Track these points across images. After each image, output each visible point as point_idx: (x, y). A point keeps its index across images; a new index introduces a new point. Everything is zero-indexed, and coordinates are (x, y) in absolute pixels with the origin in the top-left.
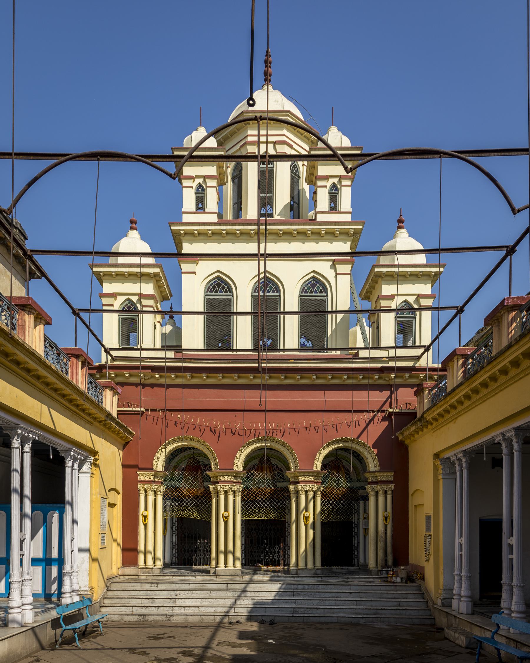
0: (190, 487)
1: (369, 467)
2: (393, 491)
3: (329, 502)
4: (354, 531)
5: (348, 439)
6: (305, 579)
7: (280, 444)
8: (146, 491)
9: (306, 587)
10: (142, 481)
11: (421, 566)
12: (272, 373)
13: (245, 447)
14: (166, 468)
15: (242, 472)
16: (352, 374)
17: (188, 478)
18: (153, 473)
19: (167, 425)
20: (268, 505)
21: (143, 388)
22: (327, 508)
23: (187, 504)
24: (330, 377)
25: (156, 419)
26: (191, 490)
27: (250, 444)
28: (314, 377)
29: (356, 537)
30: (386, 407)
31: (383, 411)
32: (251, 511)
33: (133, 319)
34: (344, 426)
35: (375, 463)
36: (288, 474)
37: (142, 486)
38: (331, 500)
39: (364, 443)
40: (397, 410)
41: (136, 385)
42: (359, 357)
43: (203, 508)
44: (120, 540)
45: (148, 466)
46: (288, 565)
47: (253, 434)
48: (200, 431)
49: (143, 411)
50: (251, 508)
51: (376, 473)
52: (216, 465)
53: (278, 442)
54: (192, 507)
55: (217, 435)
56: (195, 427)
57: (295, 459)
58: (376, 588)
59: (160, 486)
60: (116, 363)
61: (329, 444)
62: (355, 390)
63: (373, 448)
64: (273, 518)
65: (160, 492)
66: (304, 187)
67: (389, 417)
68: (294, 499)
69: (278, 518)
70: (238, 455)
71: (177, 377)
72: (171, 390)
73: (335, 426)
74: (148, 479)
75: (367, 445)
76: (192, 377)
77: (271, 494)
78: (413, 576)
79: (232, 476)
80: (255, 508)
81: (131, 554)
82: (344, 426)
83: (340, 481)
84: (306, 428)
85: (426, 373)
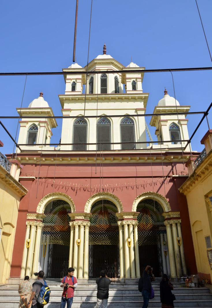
0: (59, 224)
1: (164, 210)
2: (180, 223)
3: (143, 233)
4: (159, 253)
5: (151, 193)
6: (130, 286)
7: (112, 196)
8: (31, 226)
9: (131, 292)
10: (29, 220)
11: (206, 274)
12: (106, 157)
13: (91, 198)
14: (46, 212)
15: (89, 213)
16: (150, 156)
17: (58, 219)
18: (36, 215)
19: (47, 186)
20: (105, 235)
21: (36, 166)
22: (142, 237)
23: (56, 235)
24: (138, 158)
25: (41, 183)
26: (59, 226)
27: (94, 197)
28: (130, 158)
29: (160, 257)
30: (171, 174)
31: (169, 177)
32: (95, 240)
33: (35, 133)
34: (148, 185)
35: (168, 207)
36: (117, 215)
37: (28, 222)
38: (144, 231)
39: (160, 195)
40: (177, 176)
41: (32, 164)
42: (153, 148)
43: (66, 237)
44: (10, 260)
45: (35, 211)
46: (119, 277)
47: (96, 191)
48: (66, 189)
49: (34, 178)
50: (95, 237)
51: (170, 213)
52: (74, 209)
53: (111, 195)
54: (59, 237)
55: (75, 191)
56: (63, 187)
57: (121, 205)
58: (179, 291)
59: (40, 223)
60: (23, 153)
61: (140, 196)
62: (153, 165)
63: (166, 198)
64: (108, 244)
65: (40, 226)
66: (121, 86)
67: (173, 180)
68: (121, 230)
69: (111, 243)
70: (87, 204)
71: (54, 160)
72: (51, 167)
73: (143, 186)
74: (33, 218)
75: (162, 196)
76: (63, 160)
77: (107, 228)
78: (202, 282)
79: (83, 216)
80: (98, 237)
81: (16, 269)
82: (148, 185)
83: (148, 219)
84: (126, 187)
85: (190, 155)
